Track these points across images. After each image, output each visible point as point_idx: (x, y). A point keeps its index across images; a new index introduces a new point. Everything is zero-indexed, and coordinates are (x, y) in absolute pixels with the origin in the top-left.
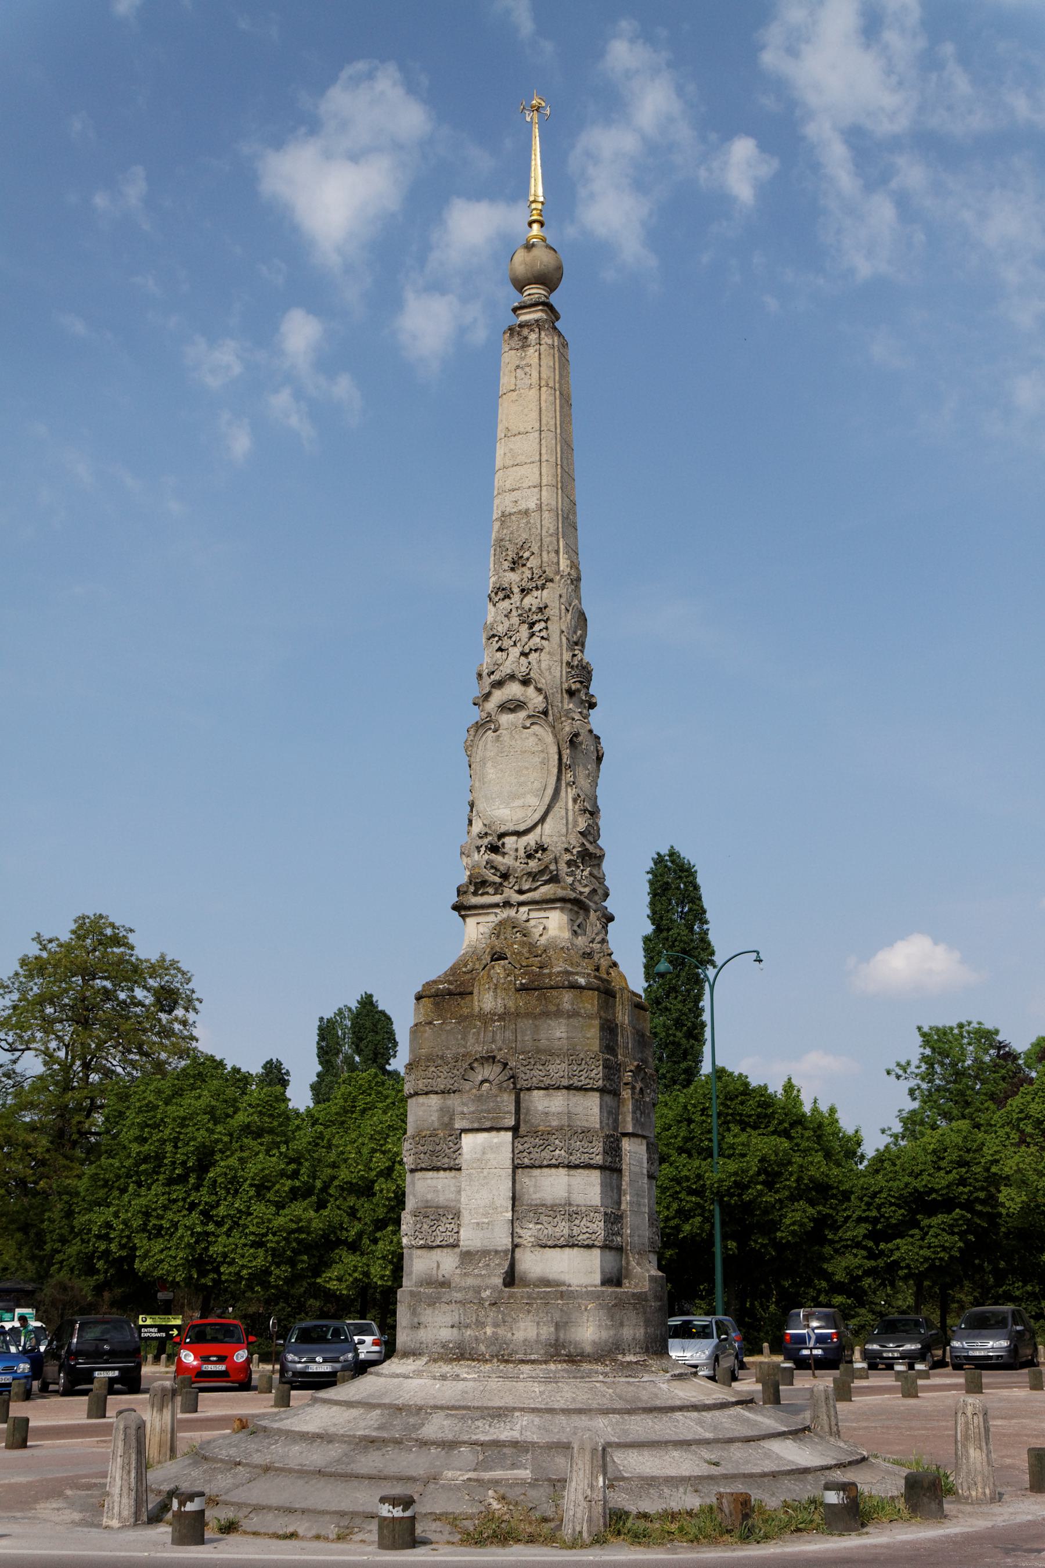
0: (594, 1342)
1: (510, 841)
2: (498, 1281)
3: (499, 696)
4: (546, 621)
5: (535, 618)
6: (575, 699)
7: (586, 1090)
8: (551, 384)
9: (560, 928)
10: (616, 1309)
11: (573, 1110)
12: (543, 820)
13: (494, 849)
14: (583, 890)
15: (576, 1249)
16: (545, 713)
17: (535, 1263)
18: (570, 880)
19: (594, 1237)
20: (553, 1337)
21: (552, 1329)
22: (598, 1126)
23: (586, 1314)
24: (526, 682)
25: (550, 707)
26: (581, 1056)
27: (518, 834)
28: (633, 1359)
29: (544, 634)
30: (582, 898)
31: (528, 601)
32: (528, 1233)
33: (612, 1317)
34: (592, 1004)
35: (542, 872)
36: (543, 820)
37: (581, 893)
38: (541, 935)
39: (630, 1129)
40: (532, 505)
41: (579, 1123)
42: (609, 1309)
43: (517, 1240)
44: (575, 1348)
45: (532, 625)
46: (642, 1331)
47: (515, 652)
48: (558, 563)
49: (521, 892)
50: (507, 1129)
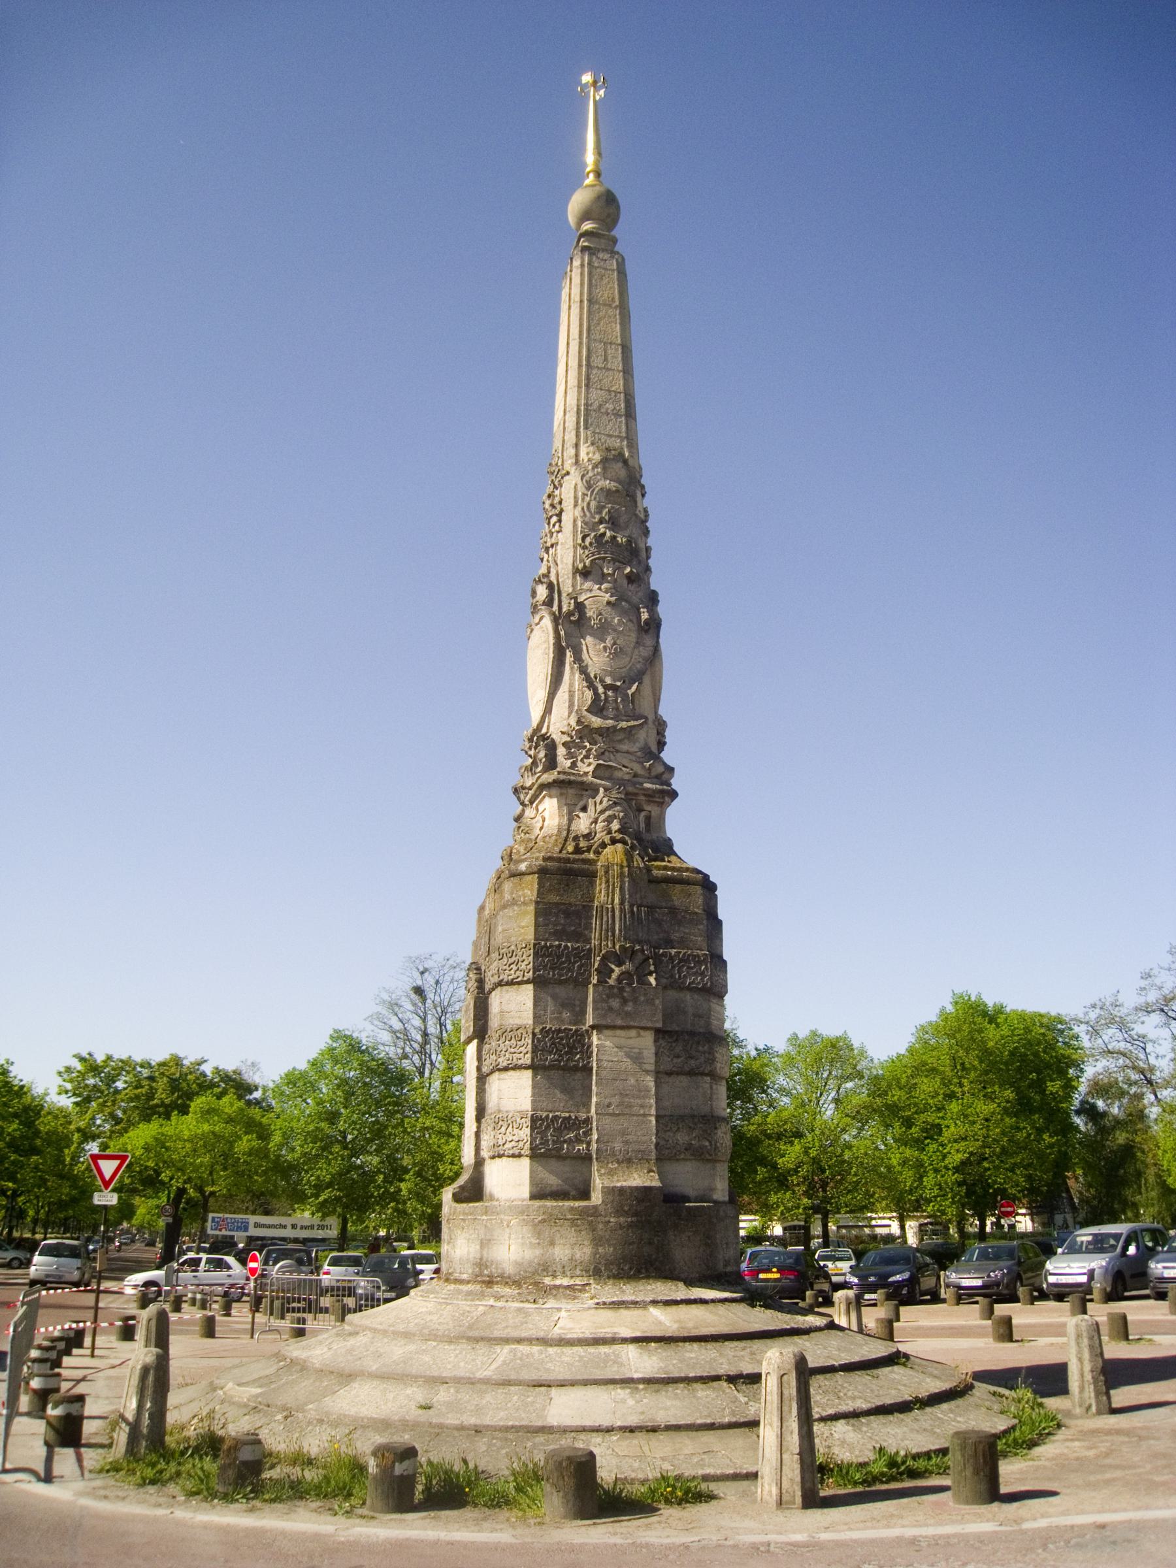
0: (516, 1263)
6: (590, 577)
7: (519, 983)
10: (543, 1226)
11: (505, 1008)
14: (587, 770)
15: (504, 1159)
18: (568, 763)
19: (521, 1144)
20: (478, 1256)
21: (478, 1247)
22: (531, 1022)
23: (507, 1230)
26: (513, 947)
28: (566, 1282)
30: (590, 778)
33: (539, 1234)
34: (532, 890)
37: (586, 774)
38: (541, 828)
41: (511, 1021)
42: (535, 1226)
44: (497, 1268)
46: (588, 1250)
48: (577, 455)
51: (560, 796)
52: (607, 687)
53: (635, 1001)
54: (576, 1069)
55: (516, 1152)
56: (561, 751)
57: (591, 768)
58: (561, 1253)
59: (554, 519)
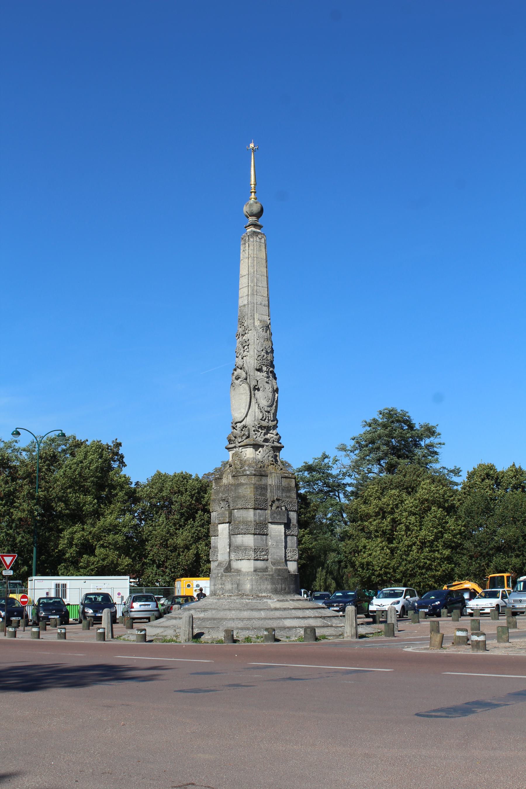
1: (238, 425)
2: (222, 571)
3: (236, 373)
4: (248, 346)
5: (244, 345)
8: (252, 255)
9: (250, 454)
12: (246, 416)
13: (234, 428)
16: (246, 379)
17: (235, 565)
18: (255, 437)
24: (241, 369)
25: (248, 377)
27: (240, 422)
29: (247, 350)
31: (244, 338)
32: (233, 556)
35: (244, 435)
36: (246, 416)
39: (270, 521)
40: (246, 302)
43: (231, 558)
45: (244, 347)
47: (240, 357)
48: (254, 323)
49: (239, 443)
50: (227, 523)
51: (253, 448)
52: (266, 412)
53: (280, 514)
54: (264, 535)
55: (249, 558)
56: (252, 433)
57: (262, 439)
58: (263, 587)
59: (246, 347)
